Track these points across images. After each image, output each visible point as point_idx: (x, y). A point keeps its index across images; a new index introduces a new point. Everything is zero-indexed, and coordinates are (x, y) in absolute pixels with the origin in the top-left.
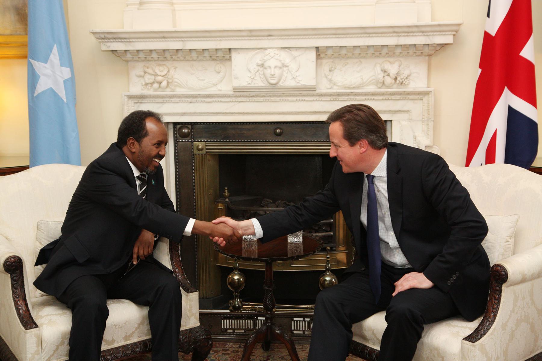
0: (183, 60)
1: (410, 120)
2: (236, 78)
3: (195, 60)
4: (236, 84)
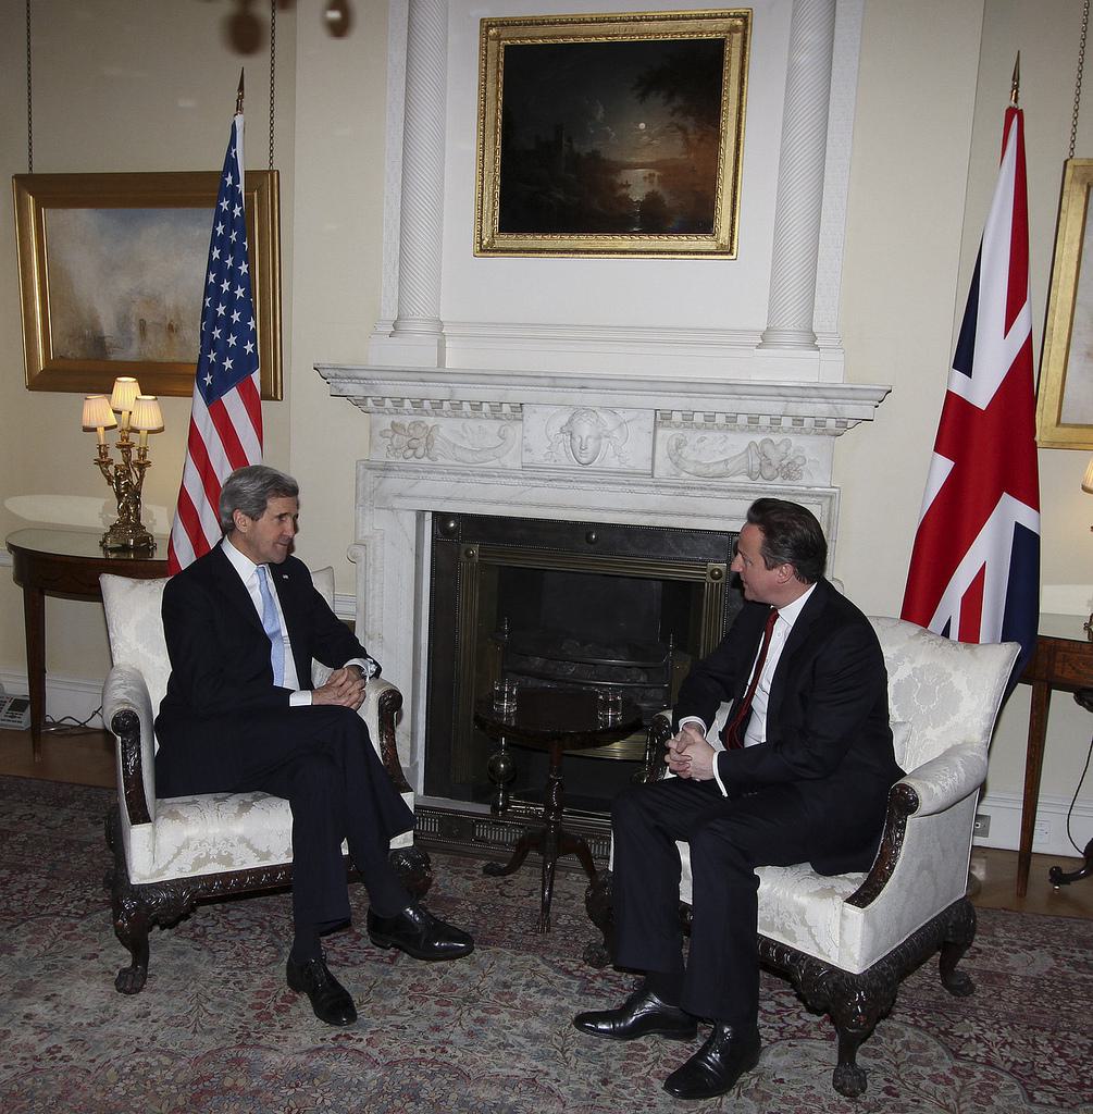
4: (527, 458)
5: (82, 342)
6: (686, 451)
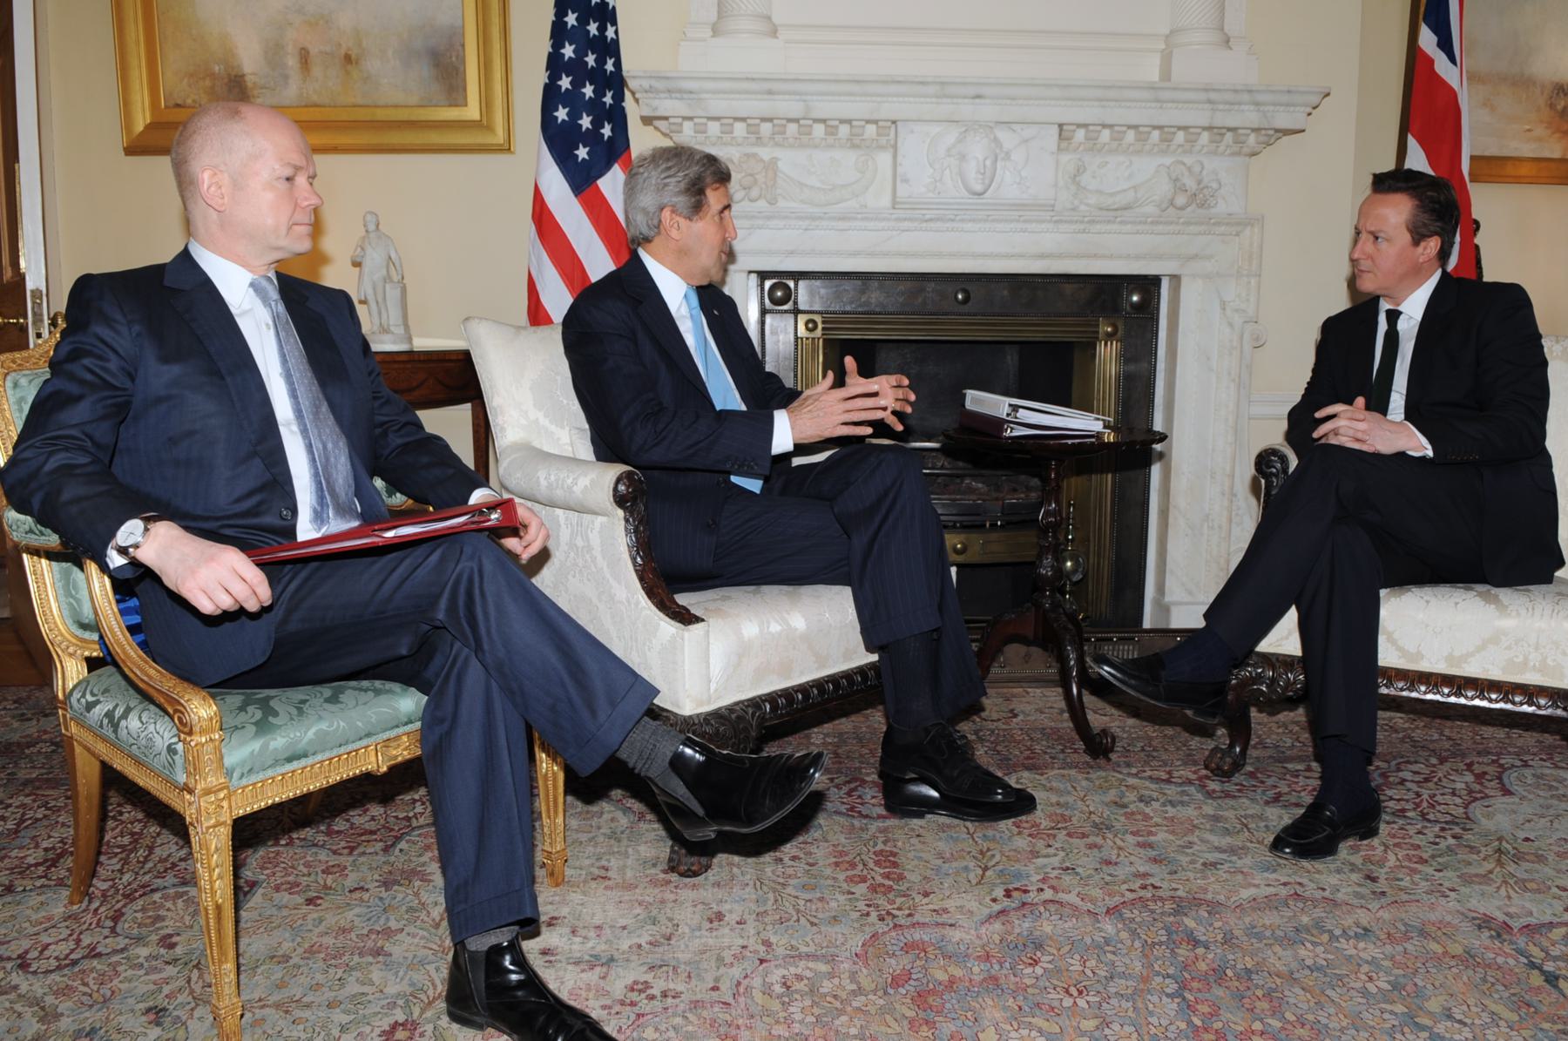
0: (792, 146)
2: (906, 181)
3: (816, 147)
5: (208, 83)
6: (1085, 179)
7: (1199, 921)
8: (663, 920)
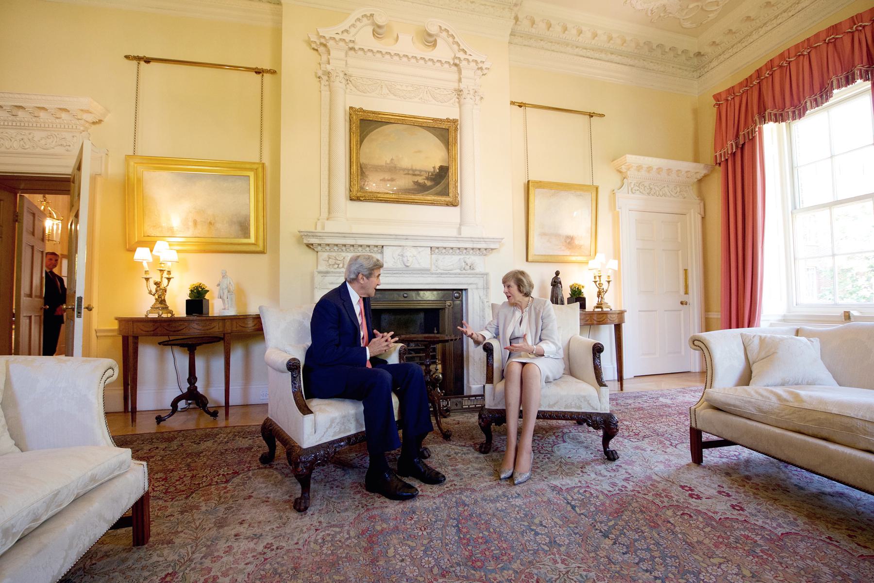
1: (477, 288)
7: (467, 497)
8: (284, 517)
